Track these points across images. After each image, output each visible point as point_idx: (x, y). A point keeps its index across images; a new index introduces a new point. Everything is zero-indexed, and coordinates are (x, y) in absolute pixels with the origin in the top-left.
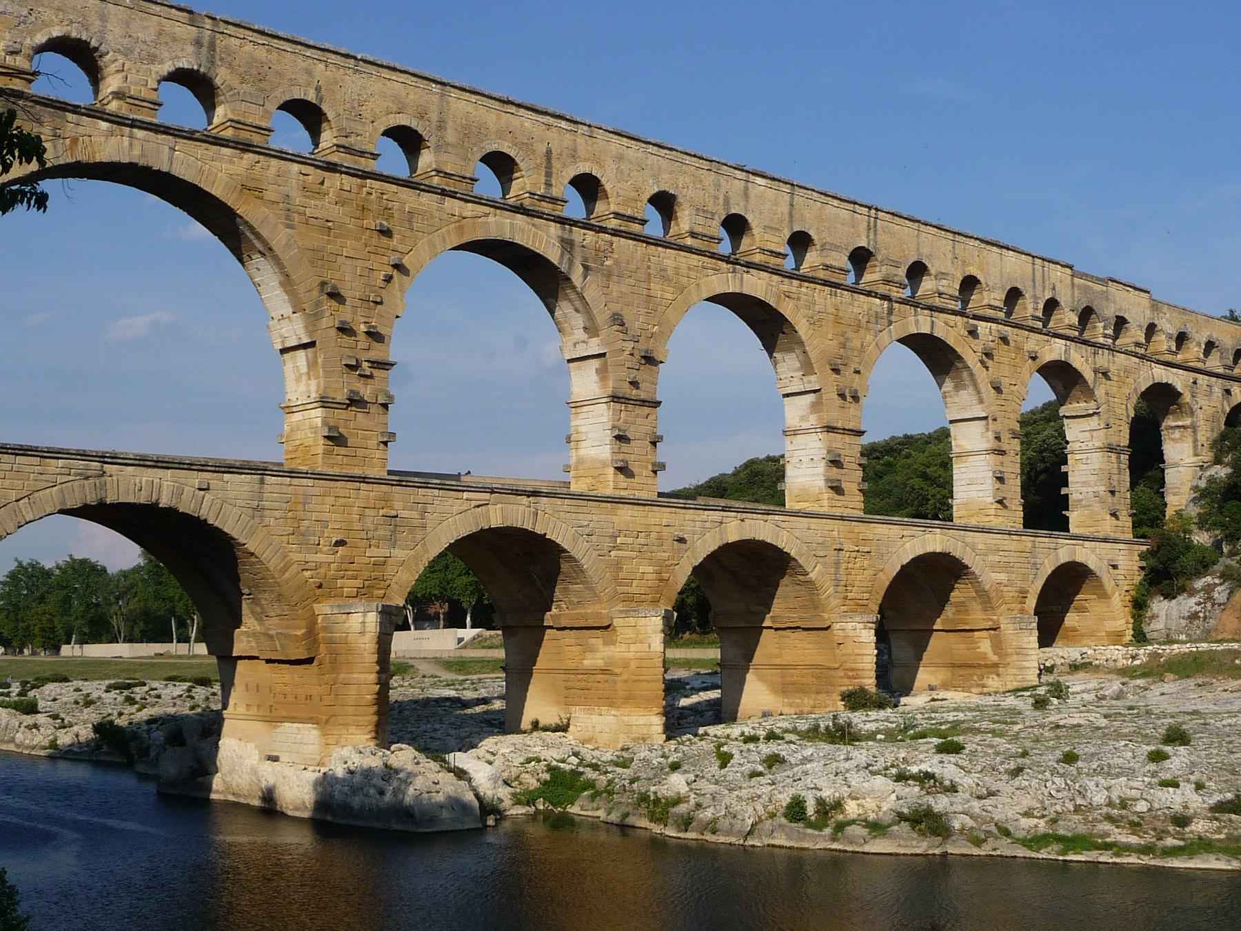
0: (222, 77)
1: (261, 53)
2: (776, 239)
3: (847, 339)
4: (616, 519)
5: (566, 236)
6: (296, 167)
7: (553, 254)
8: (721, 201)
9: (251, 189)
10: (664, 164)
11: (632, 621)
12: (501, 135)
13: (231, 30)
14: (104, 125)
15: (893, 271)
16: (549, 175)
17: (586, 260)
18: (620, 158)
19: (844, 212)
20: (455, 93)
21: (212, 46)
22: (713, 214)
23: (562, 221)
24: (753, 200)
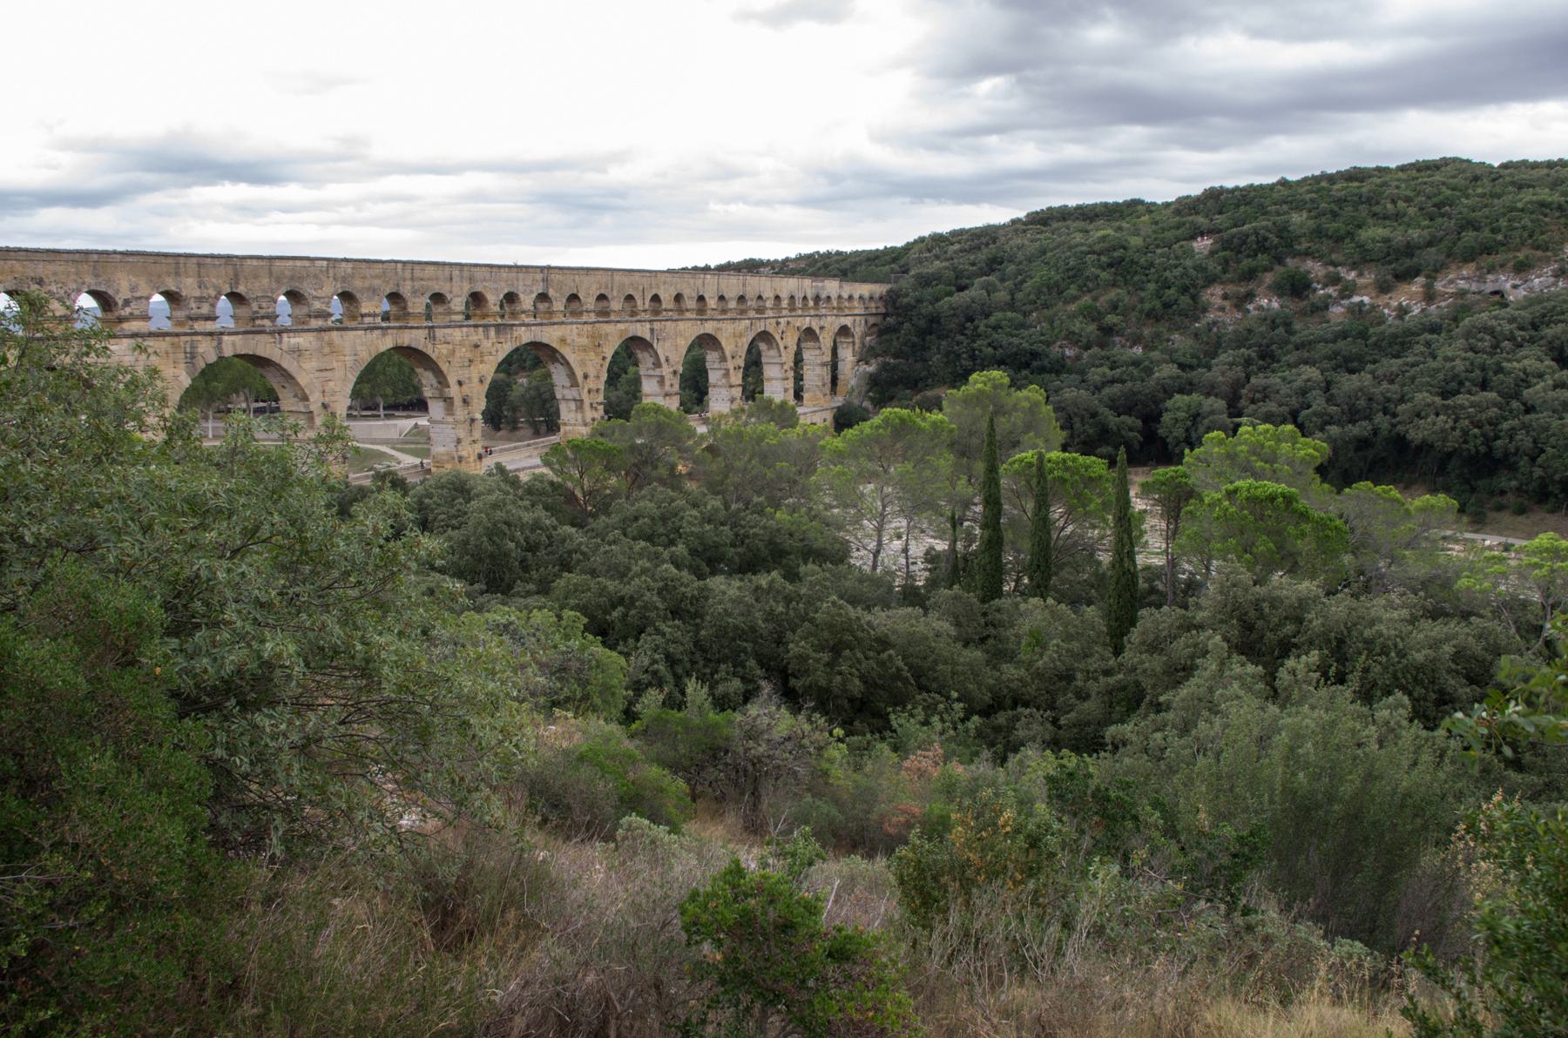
9: (563, 341)
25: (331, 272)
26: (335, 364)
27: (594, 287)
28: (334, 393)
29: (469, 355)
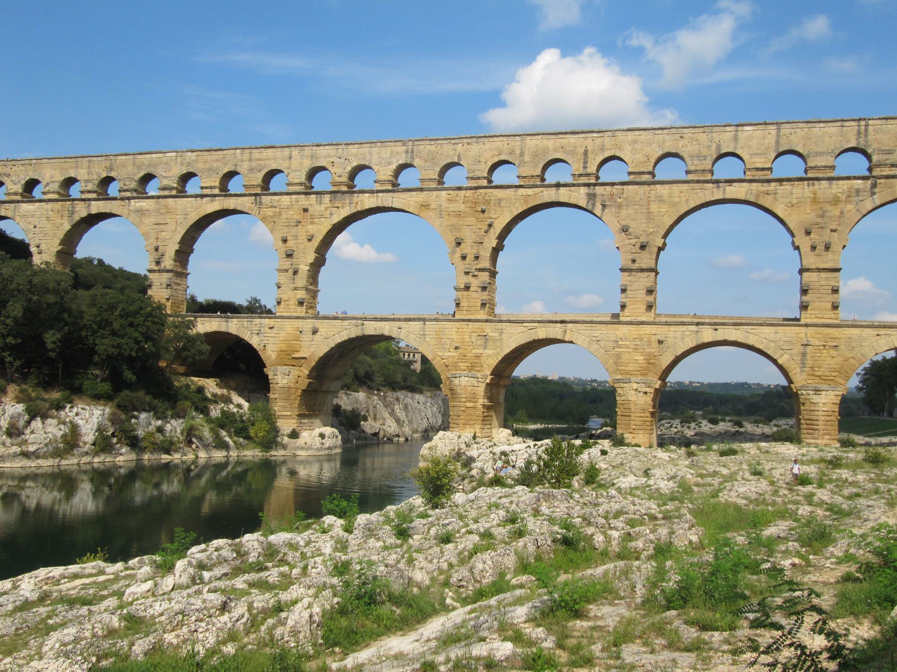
0: (416, 162)
1: (433, 148)
3: (825, 212)
4: (617, 332)
5: (591, 192)
6: (444, 192)
7: (583, 204)
8: (714, 146)
10: (668, 137)
11: (622, 385)
12: (555, 150)
13: (420, 143)
14: (367, 195)
15: (887, 157)
16: (585, 162)
17: (604, 201)
18: (635, 142)
19: (832, 129)
20: (528, 138)
21: (412, 151)
22: (705, 157)
23: (587, 185)
25: (179, 160)
26: (169, 221)
28: (165, 240)
29: (298, 217)
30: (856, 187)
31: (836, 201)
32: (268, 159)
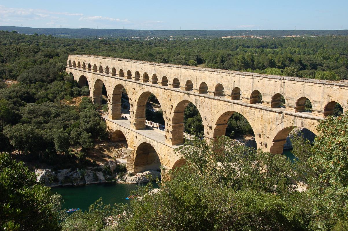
2: (247, 94)
8: (232, 84)
15: (291, 102)
18: (209, 77)
19: (272, 82)
24: (241, 82)
27: (173, 75)
30: (276, 116)
31: (269, 122)
32: (127, 66)
